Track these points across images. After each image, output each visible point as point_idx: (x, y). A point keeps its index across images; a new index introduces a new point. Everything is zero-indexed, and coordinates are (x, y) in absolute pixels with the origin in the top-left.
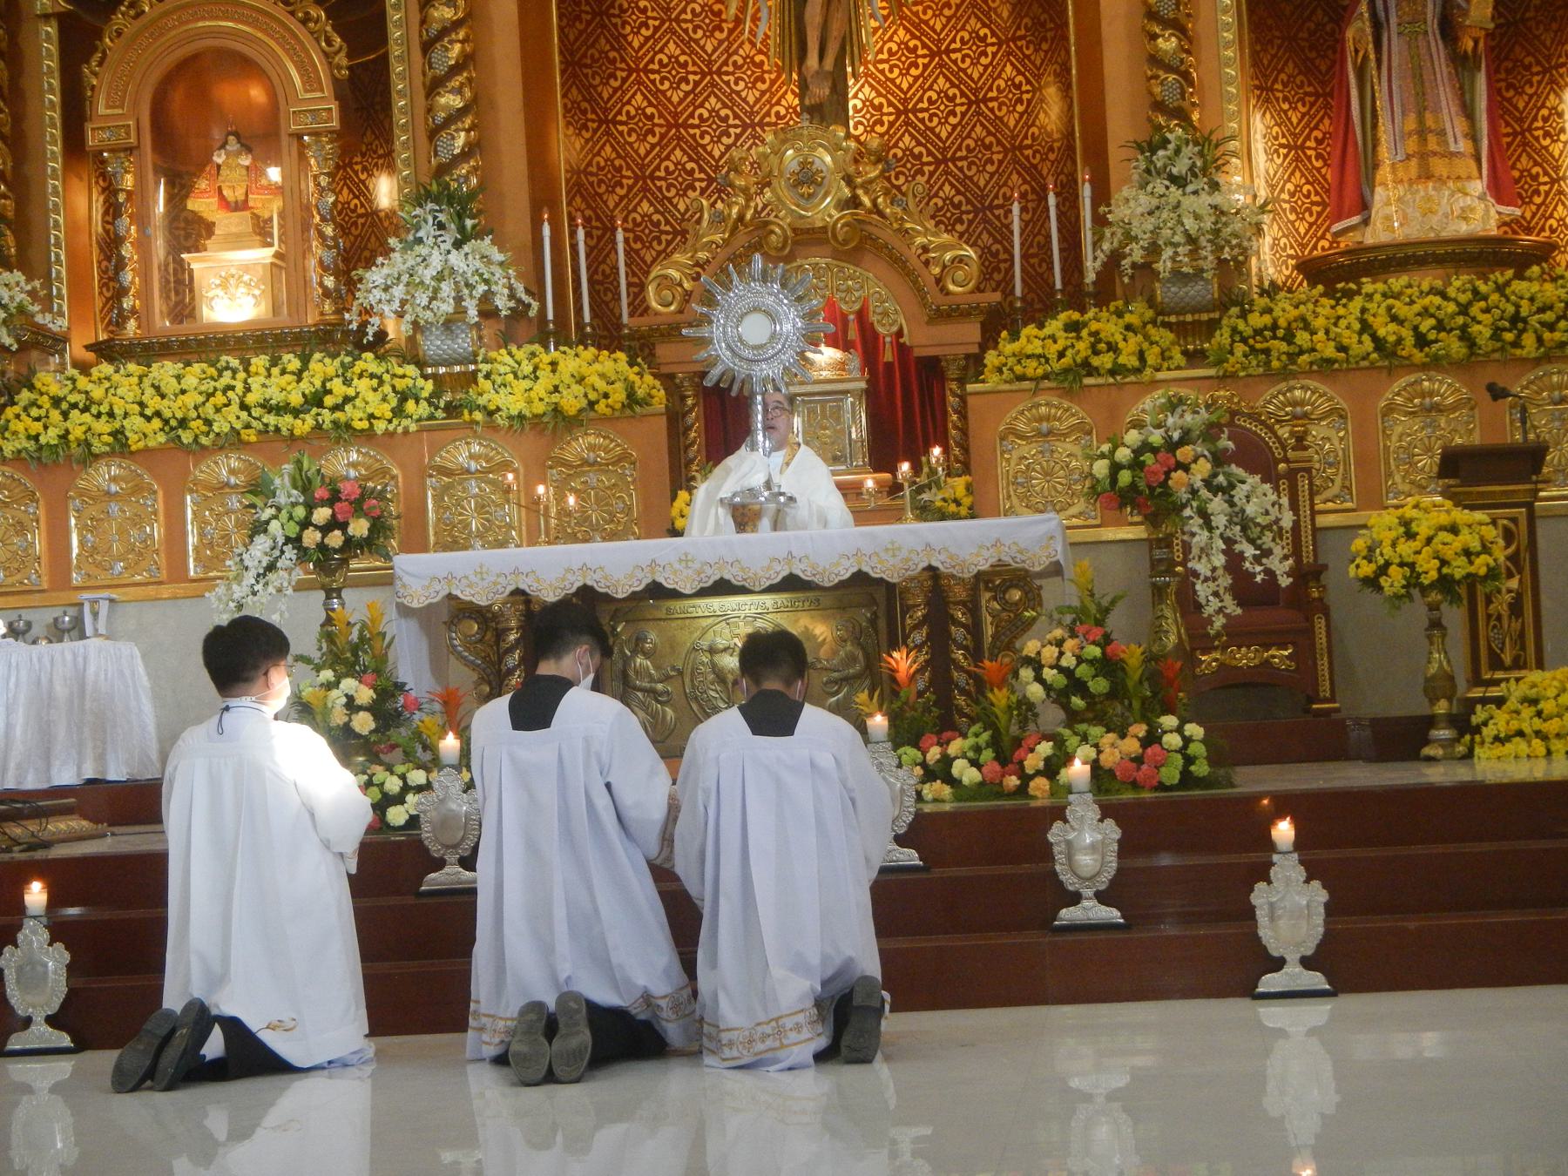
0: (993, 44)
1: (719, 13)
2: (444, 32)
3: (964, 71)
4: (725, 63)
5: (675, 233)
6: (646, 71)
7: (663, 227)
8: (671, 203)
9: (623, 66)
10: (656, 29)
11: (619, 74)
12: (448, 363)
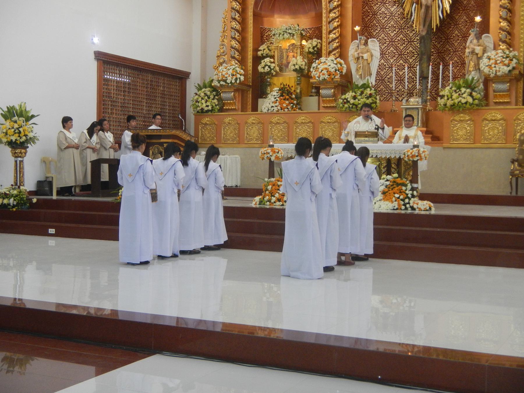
0: (468, 23)
1: (404, 14)
2: (333, 20)
3: (462, 29)
4: (405, 27)
5: (389, 67)
6: (385, 28)
7: (386, 66)
8: (389, 60)
9: (379, 27)
10: (389, 18)
11: (378, 29)
12: (326, 97)
